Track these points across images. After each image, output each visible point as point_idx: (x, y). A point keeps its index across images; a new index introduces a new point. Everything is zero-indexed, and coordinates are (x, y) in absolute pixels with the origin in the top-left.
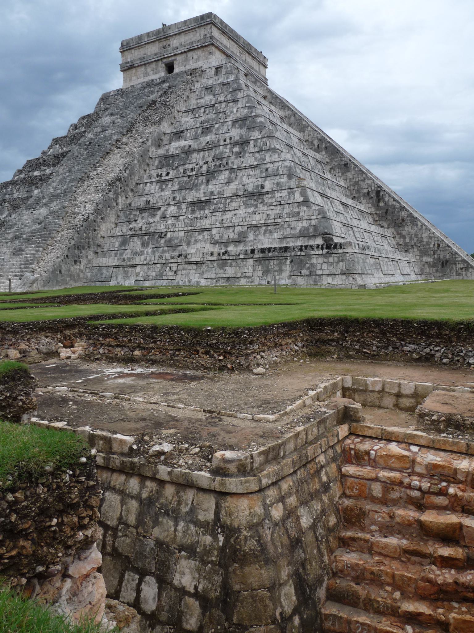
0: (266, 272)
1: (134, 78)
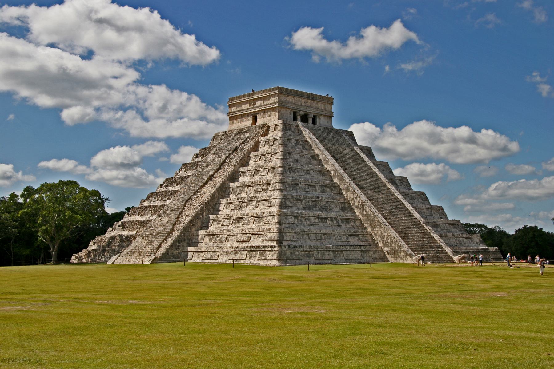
0: (251, 257)
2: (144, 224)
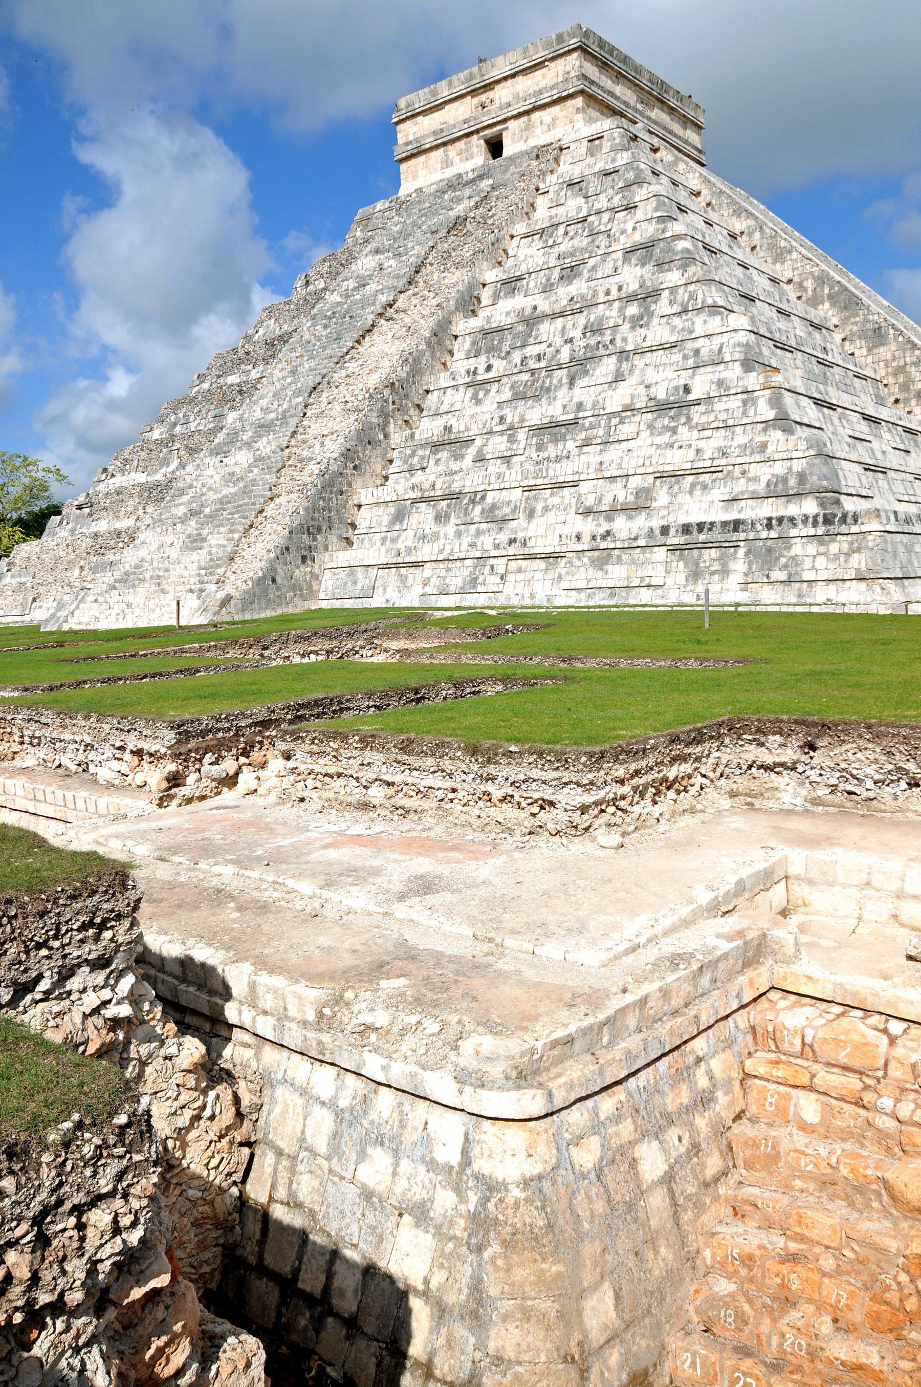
0: (695, 575)
1: (422, 172)
2: (155, 493)
